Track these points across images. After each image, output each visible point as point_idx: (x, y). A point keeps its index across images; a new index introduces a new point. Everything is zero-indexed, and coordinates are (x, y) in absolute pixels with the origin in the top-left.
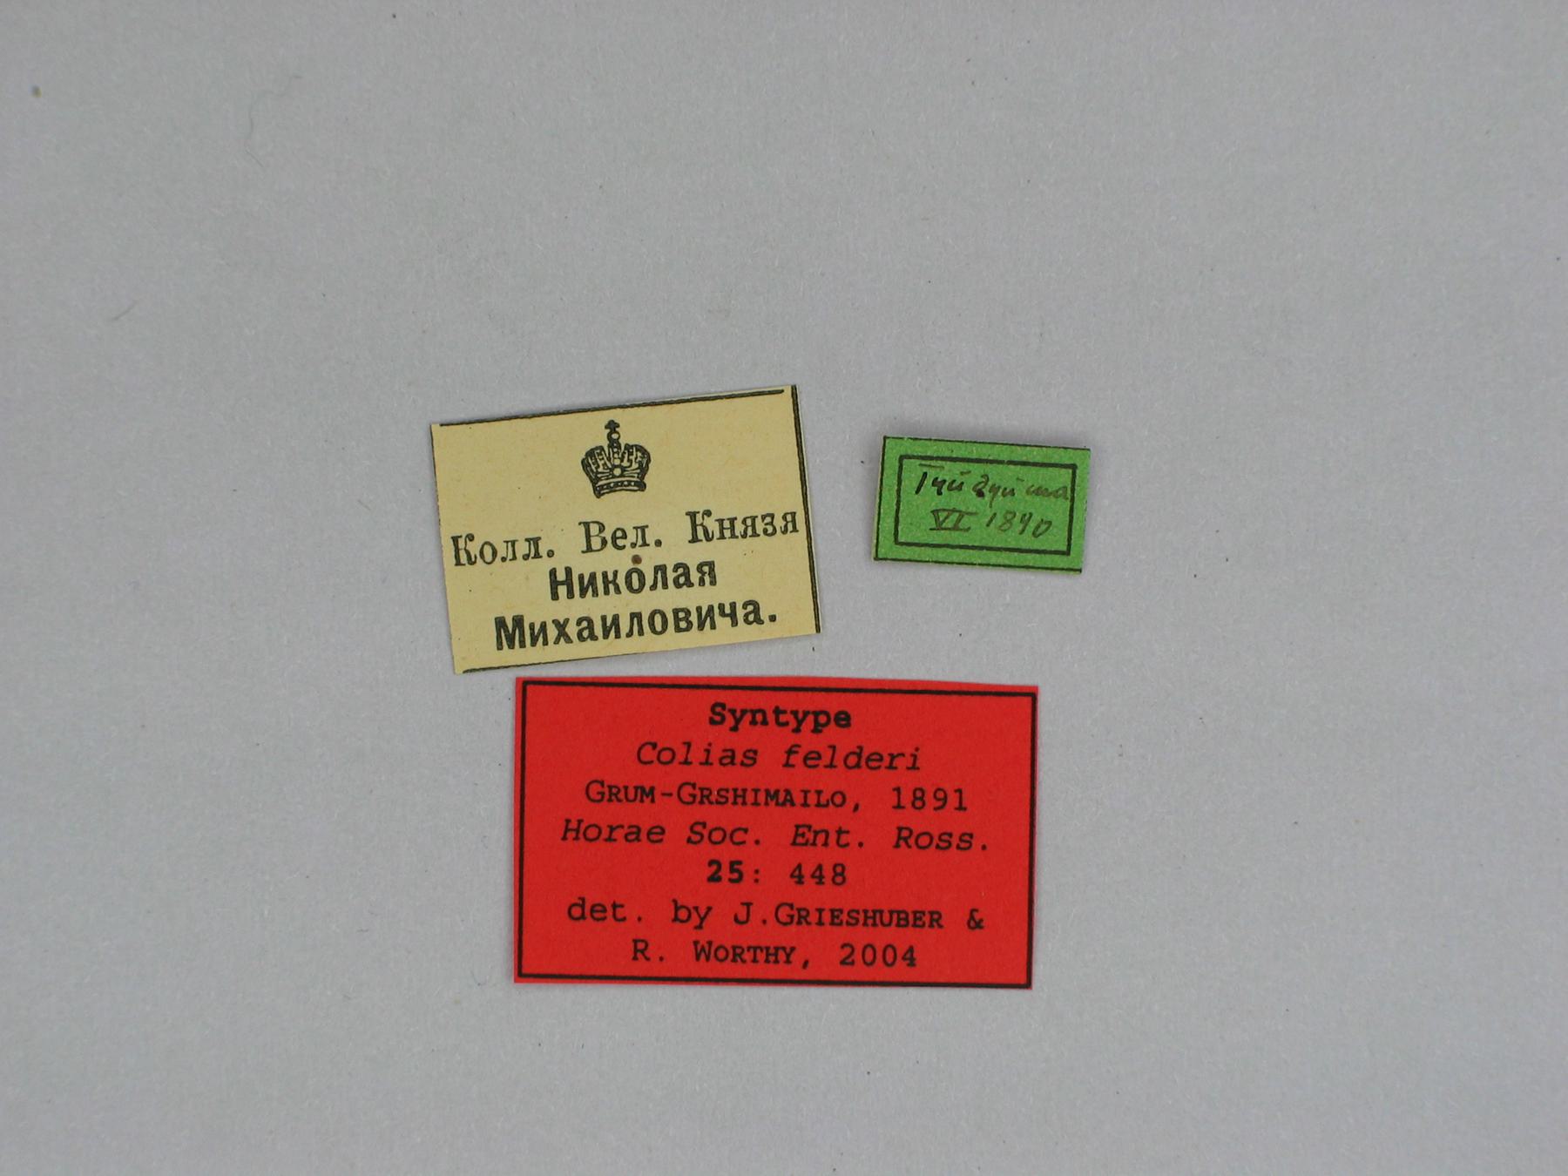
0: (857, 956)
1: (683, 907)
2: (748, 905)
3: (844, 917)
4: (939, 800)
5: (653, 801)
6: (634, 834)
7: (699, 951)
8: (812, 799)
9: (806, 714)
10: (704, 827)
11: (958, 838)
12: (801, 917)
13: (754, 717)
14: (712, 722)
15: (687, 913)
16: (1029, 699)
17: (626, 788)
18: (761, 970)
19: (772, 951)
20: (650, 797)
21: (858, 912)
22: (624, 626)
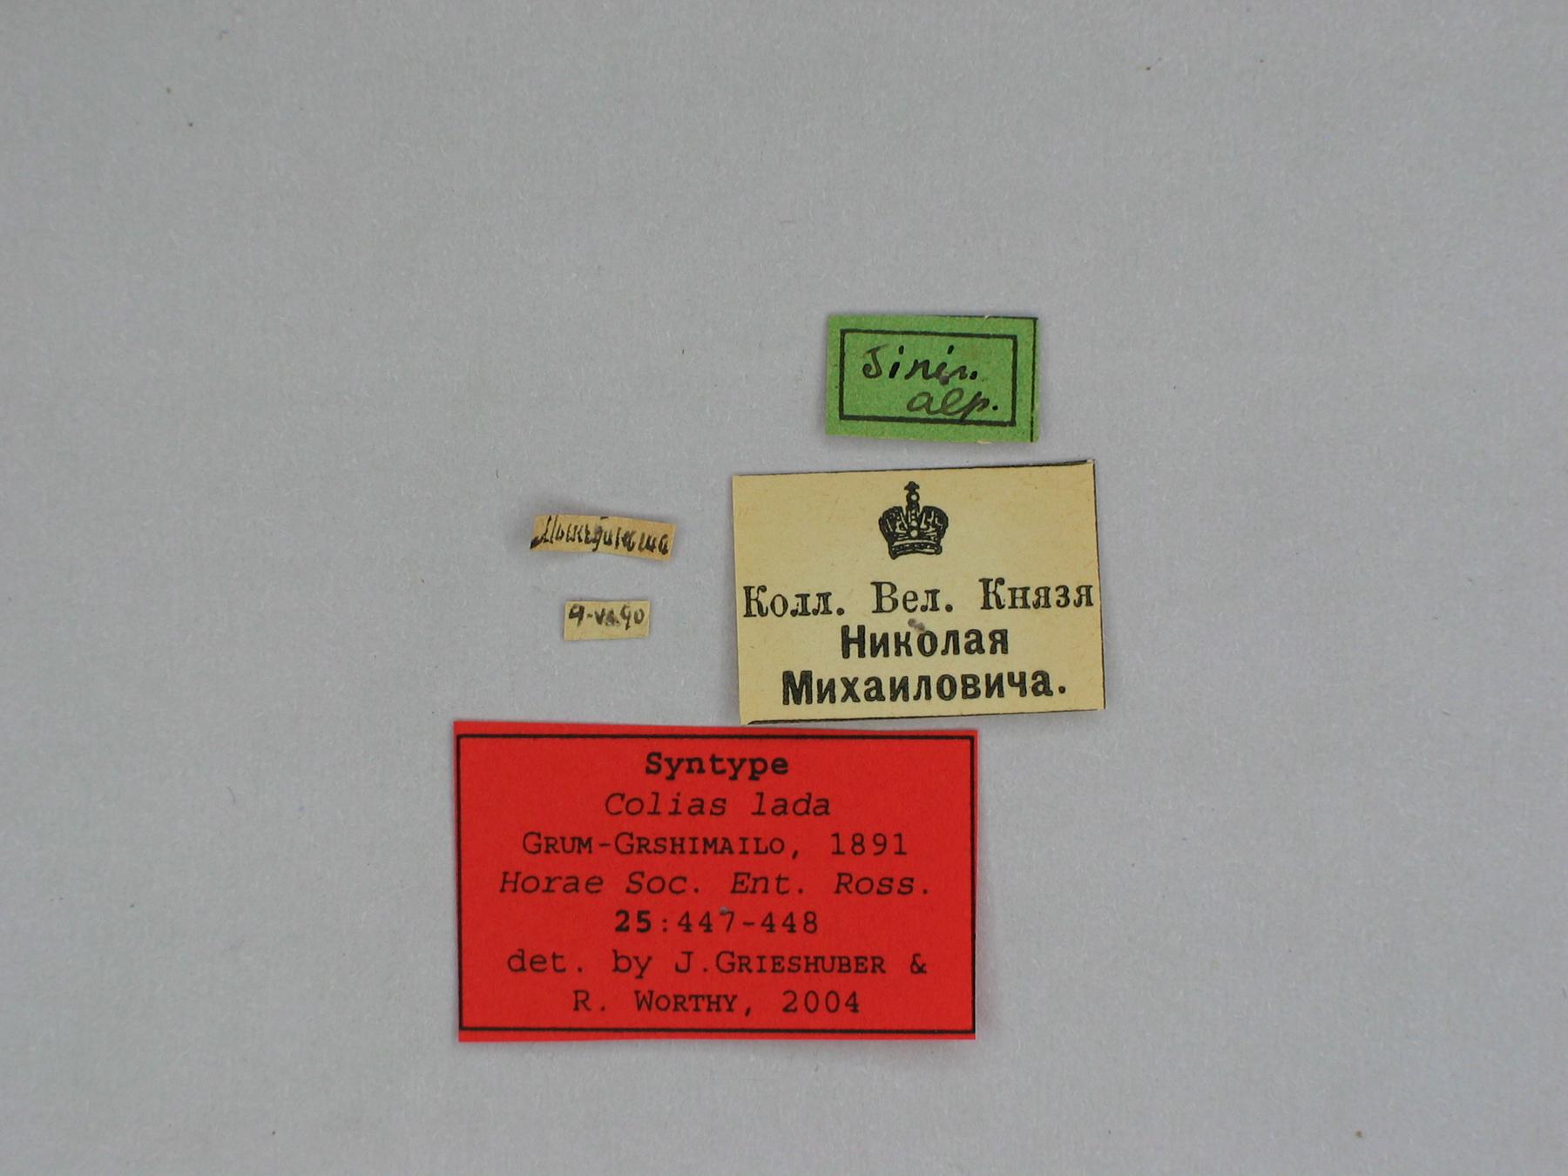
0: (800, 1002)
1: (622, 957)
2: (689, 954)
3: (786, 964)
5: (590, 852)
6: (573, 885)
7: (641, 998)
8: (751, 845)
9: (742, 761)
10: (643, 876)
11: (899, 883)
12: (743, 963)
13: (690, 765)
14: (648, 771)
17: (563, 839)
19: (714, 999)
20: (588, 849)
21: (799, 959)
22: (912, 690)
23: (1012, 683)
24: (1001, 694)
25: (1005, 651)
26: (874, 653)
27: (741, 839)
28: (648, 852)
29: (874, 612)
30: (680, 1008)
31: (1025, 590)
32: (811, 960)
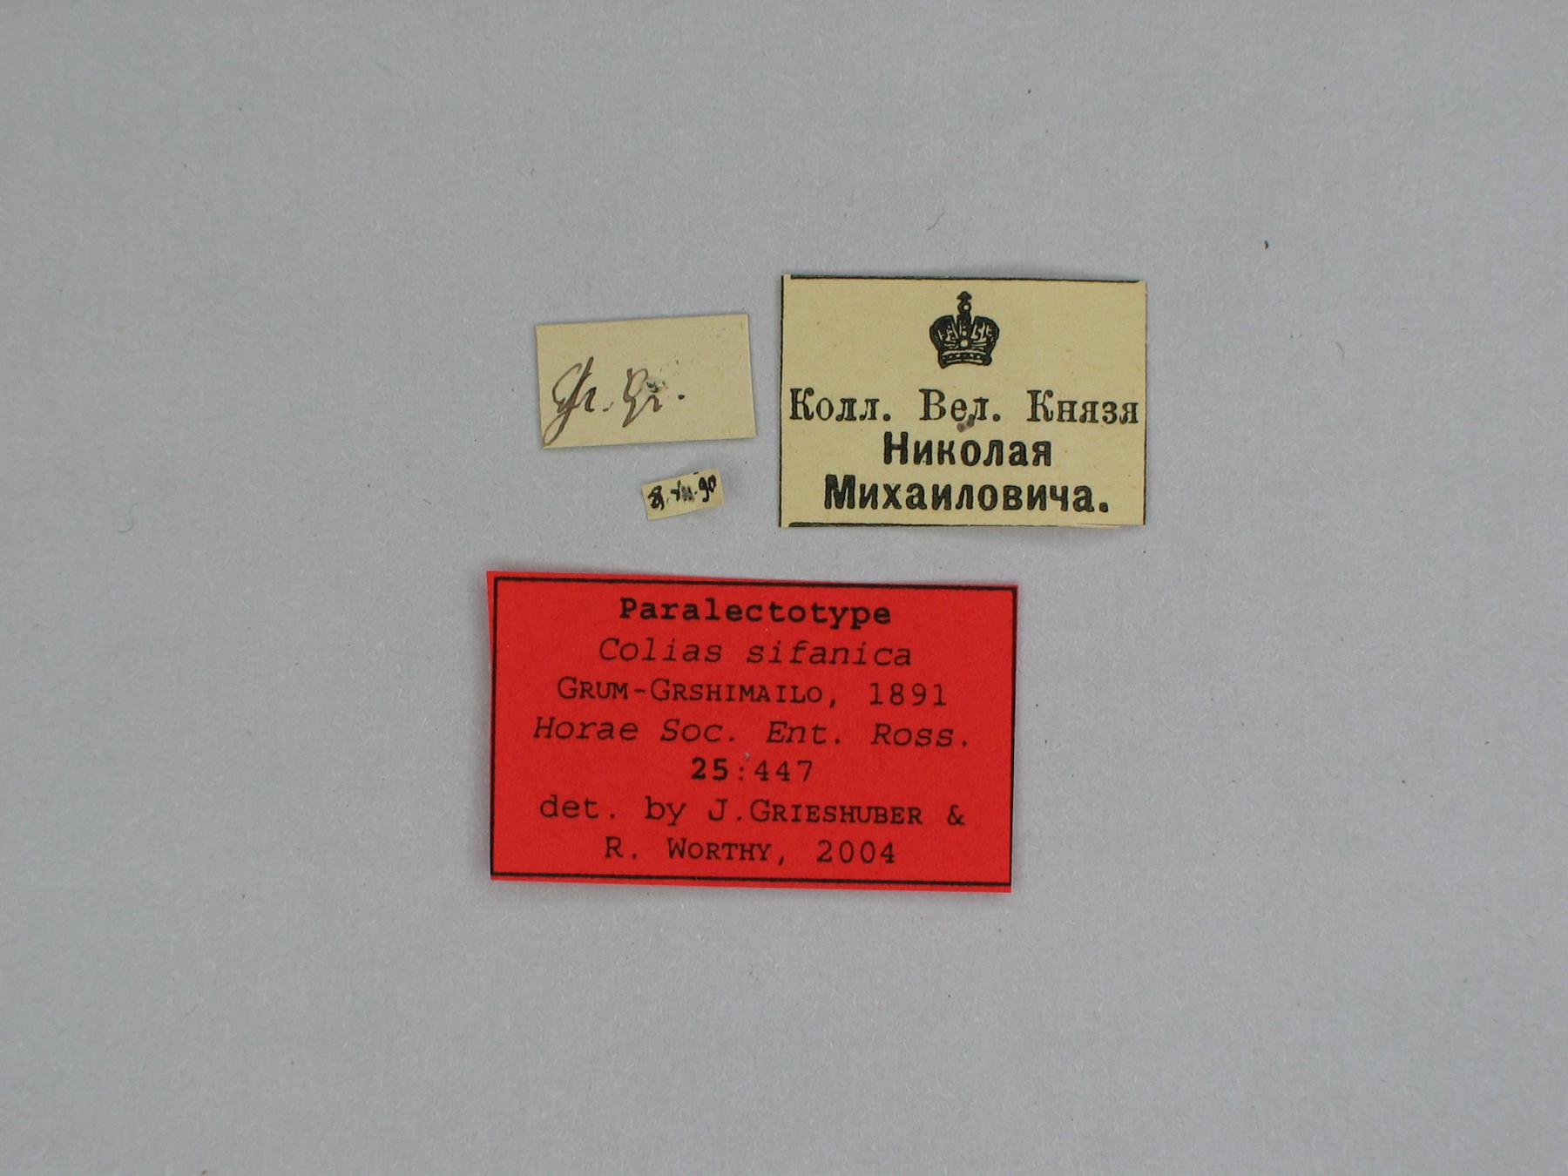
0: (834, 854)
1: (656, 804)
2: (723, 802)
3: (821, 814)
5: (626, 697)
6: (607, 731)
8: (788, 694)
12: (778, 813)
16: (1010, 593)
17: (599, 684)
18: (738, 867)
19: (747, 847)
22: (955, 499)
24: (1043, 507)
25: (1048, 463)
26: (917, 460)
27: (778, 686)
28: (684, 699)
29: (921, 419)
30: (713, 857)
31: (1073, 404)
32: (847, 810)
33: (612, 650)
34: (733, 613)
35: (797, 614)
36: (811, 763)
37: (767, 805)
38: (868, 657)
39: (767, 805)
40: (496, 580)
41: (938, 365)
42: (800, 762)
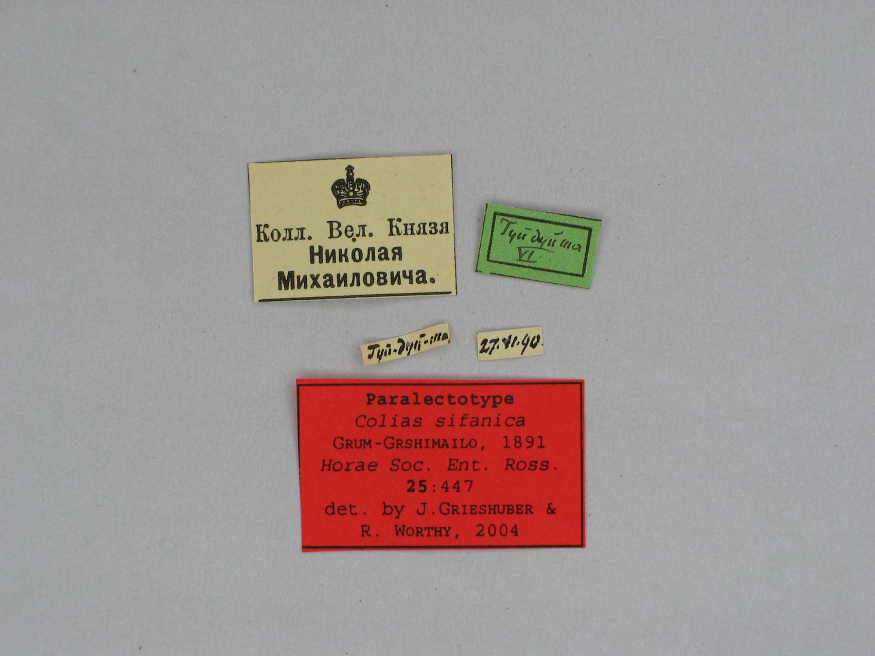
0: (486, 531)
1: (387, 506)
2: (425, 504)
3: (478, 509)
4: (529, 442)
5: (370, 447)
6: (361, 467)
7: (398, 530)
11: (540, 463)
12: (455, 510)
15: (391, 509)
16: (578, 386)
17: (355, 441)
18: (432, 540)
19: (438, 529)
22: (349, 281)
23: (405, 276)
24: (399, 283)
25: (400, 259)
26: (328, 261)
27: (453, 440)
28: (402, 447)
29: (329, 238)
31: (412, 225)
32: (492, 507)
33: (362, 421)
34: (428, 400)
35: (462, 400)
36: (472, 481)
37: (449, 505)
38: (502, 421)
39: (449, 505)
40: (298, 386)
41: (337, 207)
42: (465, 481)
